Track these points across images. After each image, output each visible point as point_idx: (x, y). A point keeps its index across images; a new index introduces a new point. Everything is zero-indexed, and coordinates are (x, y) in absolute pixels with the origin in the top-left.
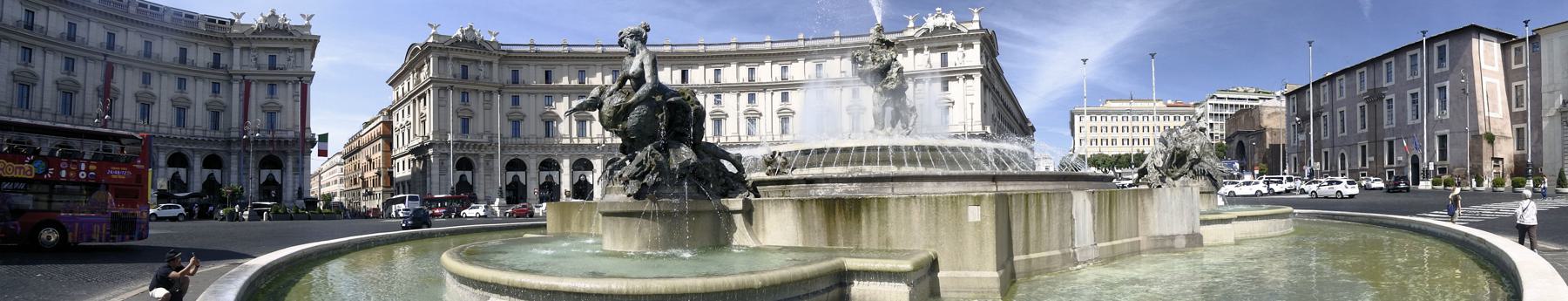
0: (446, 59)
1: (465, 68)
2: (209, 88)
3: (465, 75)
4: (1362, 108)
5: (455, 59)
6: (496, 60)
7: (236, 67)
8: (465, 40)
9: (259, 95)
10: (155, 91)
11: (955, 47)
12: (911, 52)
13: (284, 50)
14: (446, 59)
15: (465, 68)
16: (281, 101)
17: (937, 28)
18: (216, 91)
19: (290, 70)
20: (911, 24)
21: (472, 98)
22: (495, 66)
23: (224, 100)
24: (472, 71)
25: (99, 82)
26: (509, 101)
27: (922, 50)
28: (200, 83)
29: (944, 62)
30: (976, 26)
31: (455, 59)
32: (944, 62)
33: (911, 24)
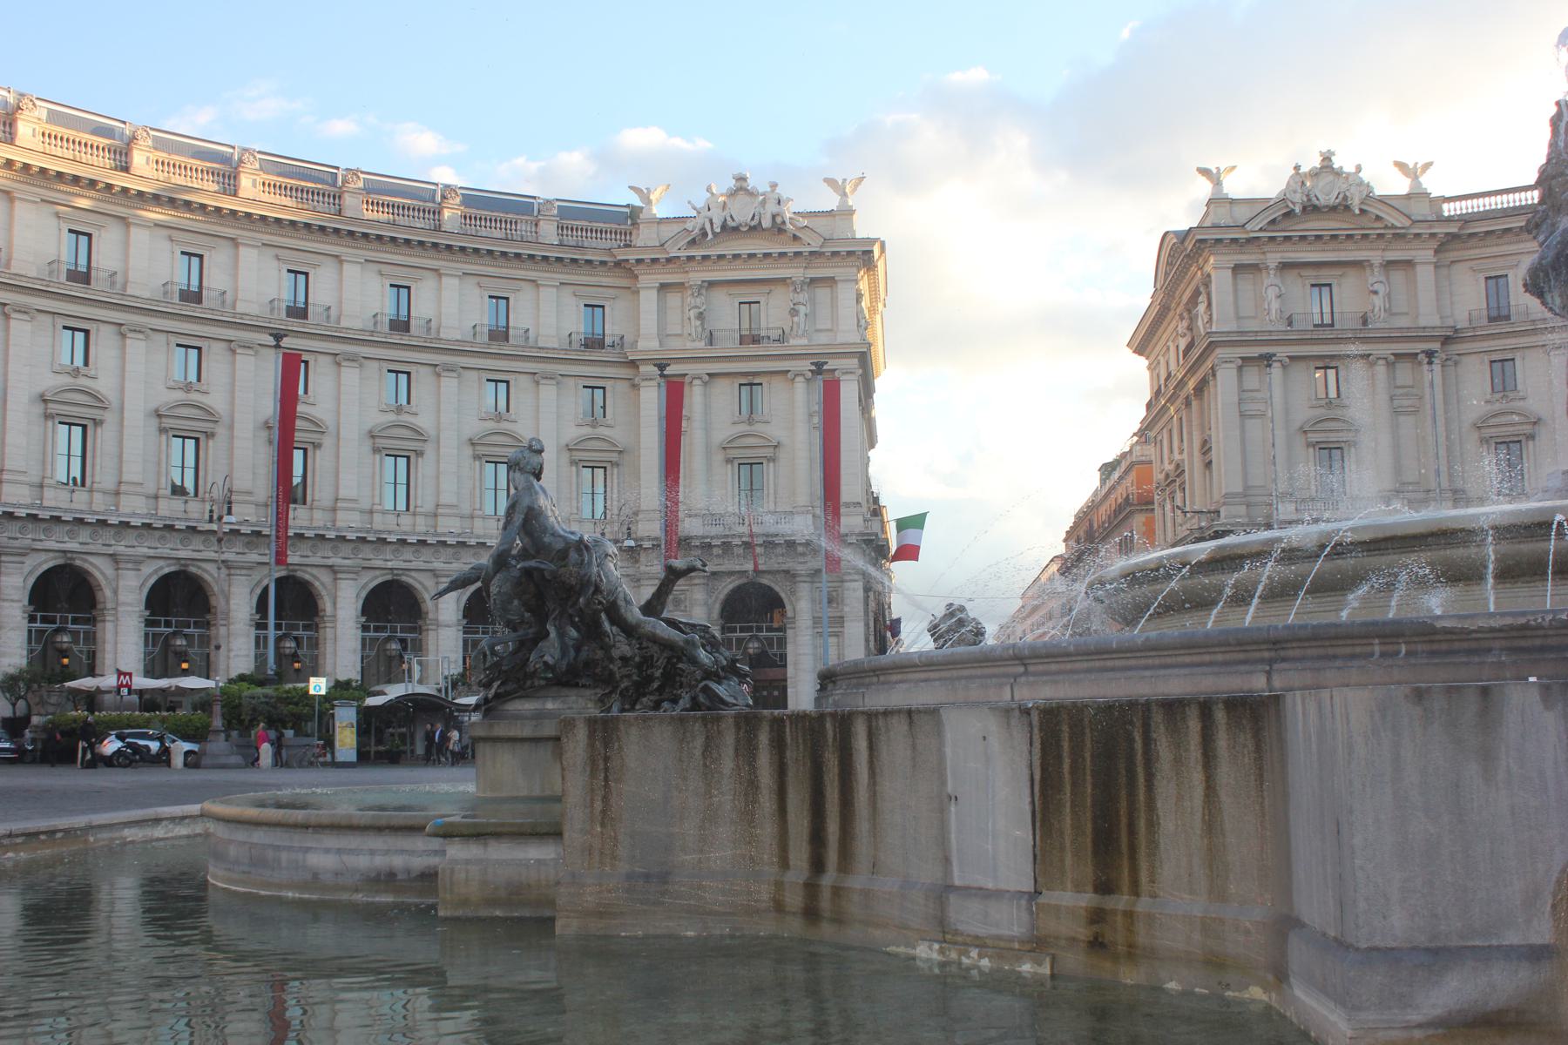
0: (1255, 268)
2: (575, 401)
5: (1285, 266)
6: (1424, 254)
7: (648, 344)
8: (1311, 209)
9: (712, 414)
10: (424, 421)
13: (775, 292)
14: (1255, 268)
16: (775, 431)
18: (595, 417)
19: (797, 343)
22: (1425, 275)
23: (617, 434)
25: (269, 407)
26: (1475, 384)
28: (548, 391)
31: (1285, 266)
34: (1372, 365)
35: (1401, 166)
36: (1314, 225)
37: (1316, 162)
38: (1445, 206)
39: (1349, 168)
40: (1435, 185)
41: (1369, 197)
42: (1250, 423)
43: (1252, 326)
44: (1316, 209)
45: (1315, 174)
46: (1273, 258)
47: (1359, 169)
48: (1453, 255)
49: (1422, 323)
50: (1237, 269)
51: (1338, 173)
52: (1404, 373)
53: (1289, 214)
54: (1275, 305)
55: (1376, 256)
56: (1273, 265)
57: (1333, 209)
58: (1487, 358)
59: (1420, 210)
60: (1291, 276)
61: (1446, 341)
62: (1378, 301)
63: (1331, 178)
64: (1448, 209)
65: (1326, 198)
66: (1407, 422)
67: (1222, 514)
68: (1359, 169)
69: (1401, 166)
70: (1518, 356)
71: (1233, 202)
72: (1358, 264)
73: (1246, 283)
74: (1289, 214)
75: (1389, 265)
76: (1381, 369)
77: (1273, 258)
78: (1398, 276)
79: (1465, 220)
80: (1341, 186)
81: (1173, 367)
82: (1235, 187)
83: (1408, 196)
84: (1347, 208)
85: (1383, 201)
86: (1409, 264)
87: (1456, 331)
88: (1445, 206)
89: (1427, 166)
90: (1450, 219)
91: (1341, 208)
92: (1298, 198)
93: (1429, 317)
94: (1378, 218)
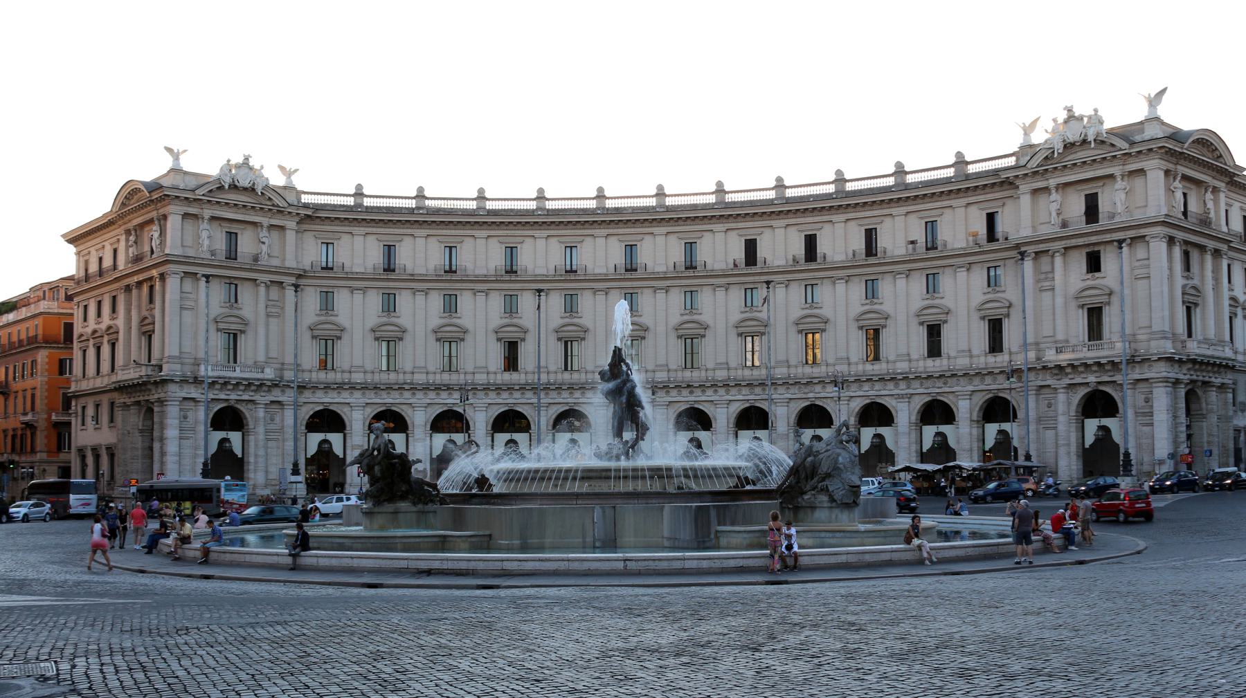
1: (232, 237)
3: (232, 254)
6: (291, 224)
8: (234, 187)
12: (1026, 200)
15: (232, 237)
21: (245, 293)
22: (290, 236)
24: (247, 244)
27: (1046, 190)
31: (213, 218)
34: (257, 285)
35: (282, 168)
36: (233, 197)
37: (241, 160)
38: (303, 196)
39: (257, 167)
40: (300, 183)
41: (267, 187)
42: (185, 313)
43: (191, 253)
44: (236, 187)
45: (238, 166)
46: (207, 213)
47: (262, 167)
48: (305, 227)
49: (287, 264)
50: (186, 216)
51: (251, 169)
52: (274, 293)
53: (221, 188)
54: (206, 242)
55: (266, 221)
56: (207, 217)
57: (245, 189)
58: (319, 290)
59: (291, 198)
60: (216, 223)
61: (299, 276)
62: (264, 248)
63: (247, 170)
64: (305, 199)
65: (244, 183)
66: (273, 321)
67: (165, 367)
68: (262, 167)
69: (282, 168)
70: (335, 290)
71: (186, 173)
72: (254, 224)
73: (189, 224)
74: (221, 188)
75: (272, 227)
76: (262, 289)
77: (207, 213)
78: (275, 234)
79: (318, 208)
80: (251, 176)
81: (108, 262)
82: (187, 165)
83: (285, 188)
84: (253, 190)
85: (274, 190)
86: (282, 228)
87: (305, 271)
88: (303, 196)
89: (296, 170)
90: (306, 206)
91: (252, 190)
92: (227, 181)
93: (290, 263)
94: (270, 199)
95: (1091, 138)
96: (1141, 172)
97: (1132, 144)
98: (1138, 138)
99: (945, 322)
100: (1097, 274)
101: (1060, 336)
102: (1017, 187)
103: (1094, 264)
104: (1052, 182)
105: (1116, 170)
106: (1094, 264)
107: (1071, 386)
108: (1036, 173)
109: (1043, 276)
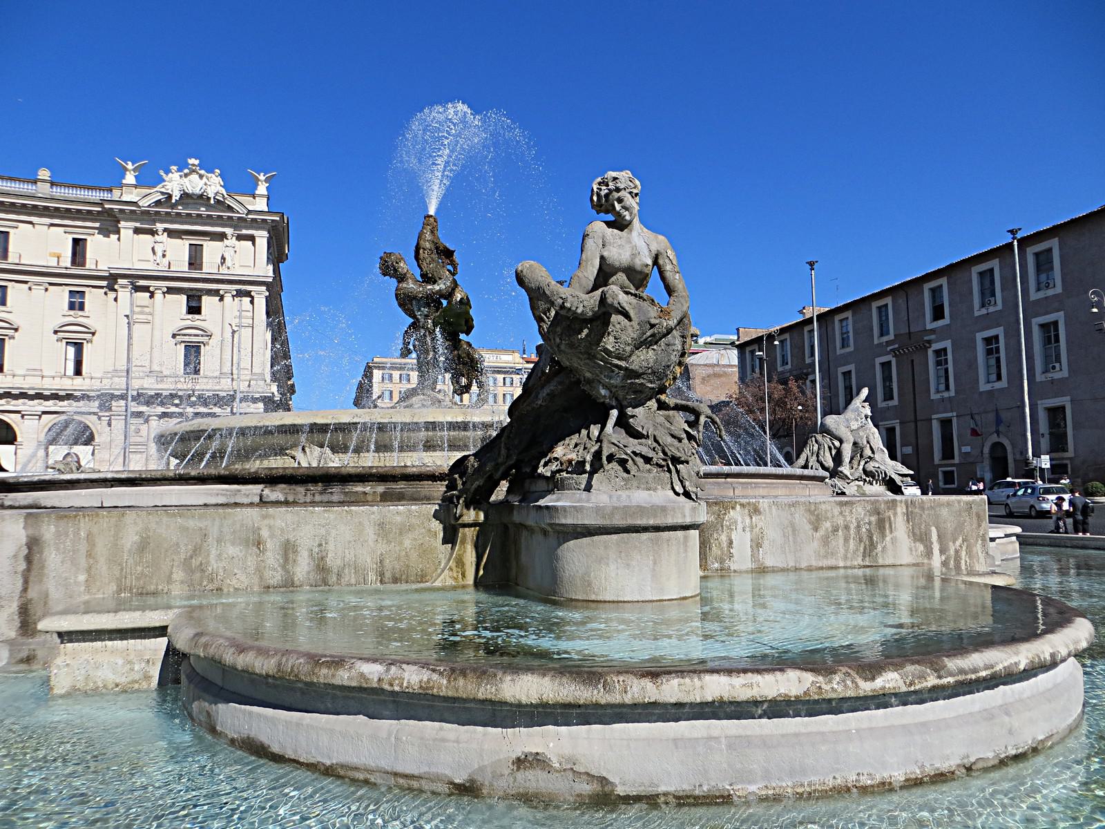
4: (886, 366)
11: (222, 237)
17: (185, 196)
20: (130, 178)
27: (153, 233)
29: (195, 260)
30: (261, 204)
32: (195, 260)
33: (130, 178)
95: (211, 195)
96: (252, 239)
97: (250, 212)
98: (250, 208)
99: (12, 337)
100: (197, 317)
101: (155, 368)
102: (118, 222)
103: (194, 310)
104: (160, 226)
105: (229, 231)
106: (194, 310)
107: (164, 415)
108: (144, 213)
109: (139, 309)
